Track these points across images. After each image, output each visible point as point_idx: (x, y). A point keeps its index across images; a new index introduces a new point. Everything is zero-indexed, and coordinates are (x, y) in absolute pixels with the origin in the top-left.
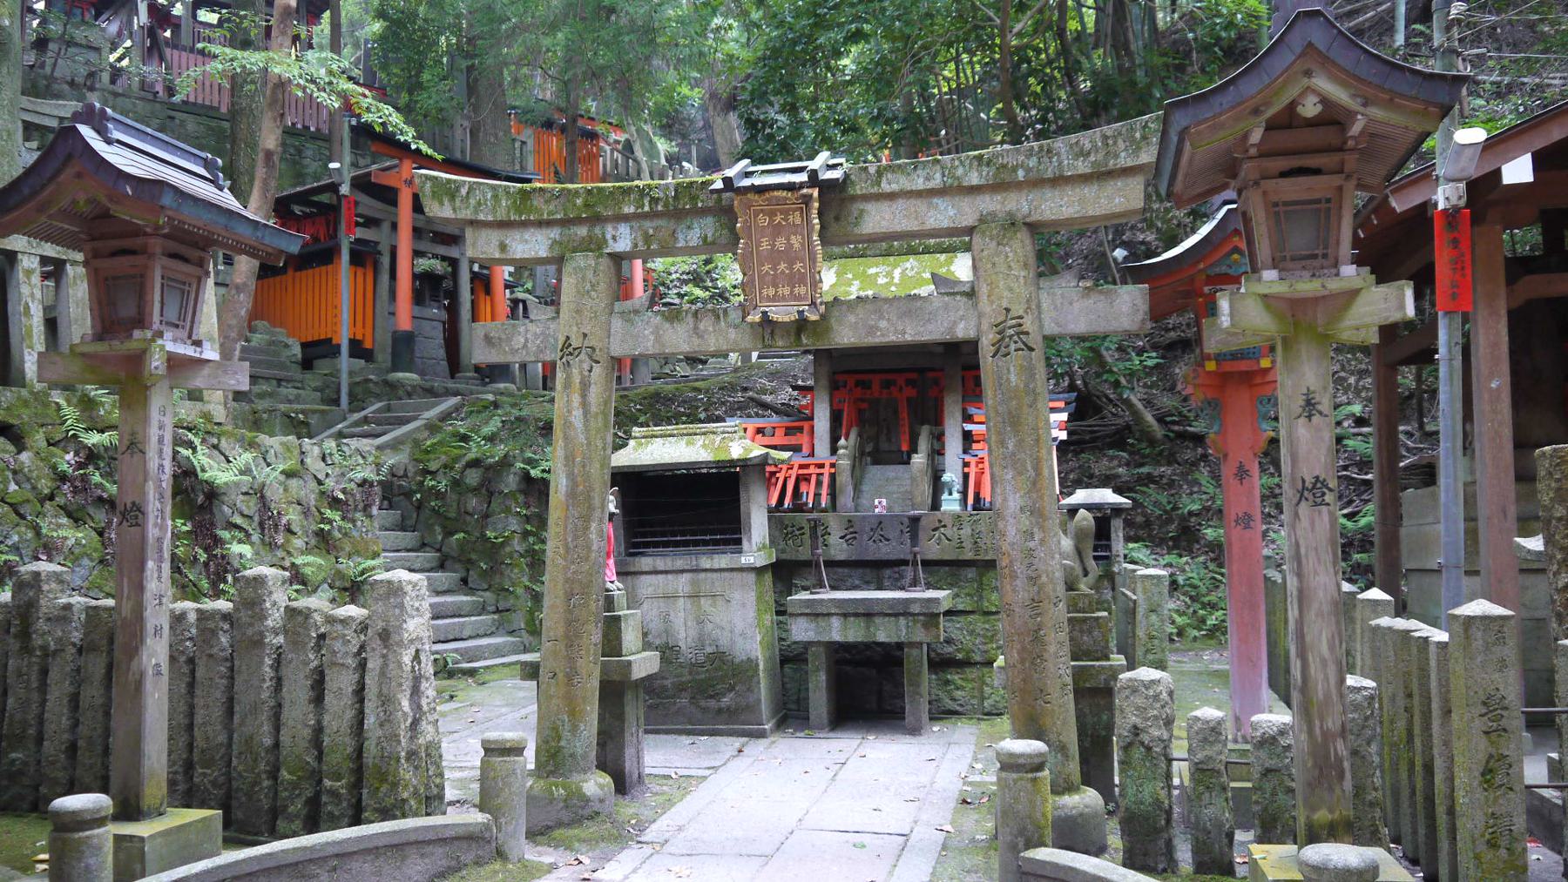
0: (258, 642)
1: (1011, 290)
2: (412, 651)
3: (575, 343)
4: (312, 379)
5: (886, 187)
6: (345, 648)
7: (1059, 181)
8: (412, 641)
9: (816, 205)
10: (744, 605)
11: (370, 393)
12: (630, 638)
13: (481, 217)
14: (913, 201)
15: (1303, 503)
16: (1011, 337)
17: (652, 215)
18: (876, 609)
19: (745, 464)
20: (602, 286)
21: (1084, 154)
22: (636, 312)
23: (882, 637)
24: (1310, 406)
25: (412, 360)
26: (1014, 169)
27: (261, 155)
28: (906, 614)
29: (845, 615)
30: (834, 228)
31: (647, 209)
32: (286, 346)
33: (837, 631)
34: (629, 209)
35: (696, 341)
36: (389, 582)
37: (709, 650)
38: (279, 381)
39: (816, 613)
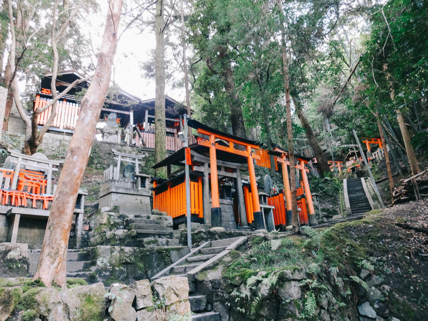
4: (177, 234)
11: (202, 239)
25: (221, 221)
32: (166, 219)
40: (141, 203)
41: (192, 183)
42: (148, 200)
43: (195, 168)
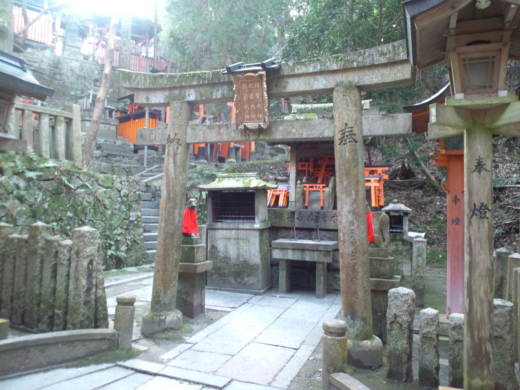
0: (35, 252)
1: (348, 115)
2: (88, 260)
3: (172, 137)
4: (136, 157)
5: (297, 72)
6: (64, 256)
7: (372, 67)
8: (88, 256)
9: (265, 79)
10: (255, 243)
11: (154, 161)
12: (200, 255)
13: (140, 87)
14: (308, 77)
15: (474, 217)
16: (347, 136)
17: (203, 85)
18: (306, 248)
19: (256, 189)
20: (184, 114)
21: (383, 54)
22: (197, 125)
23: (307, 259)
24: (479, 166)
26: (352, 62)
27: (104, 75)
28: (317, 250)
29: (294, 249)
30: (275, 90)
31: (201, 83)
32: (129, 145)
33: (291, 255)
34: (195, 83)
35: (219, 137)
36: (80, 231)
37: (241, 260)
38: (124, 157)
39: (283, 248)
40: (109, 130)
41: (151, 119)
42: (114, 128)
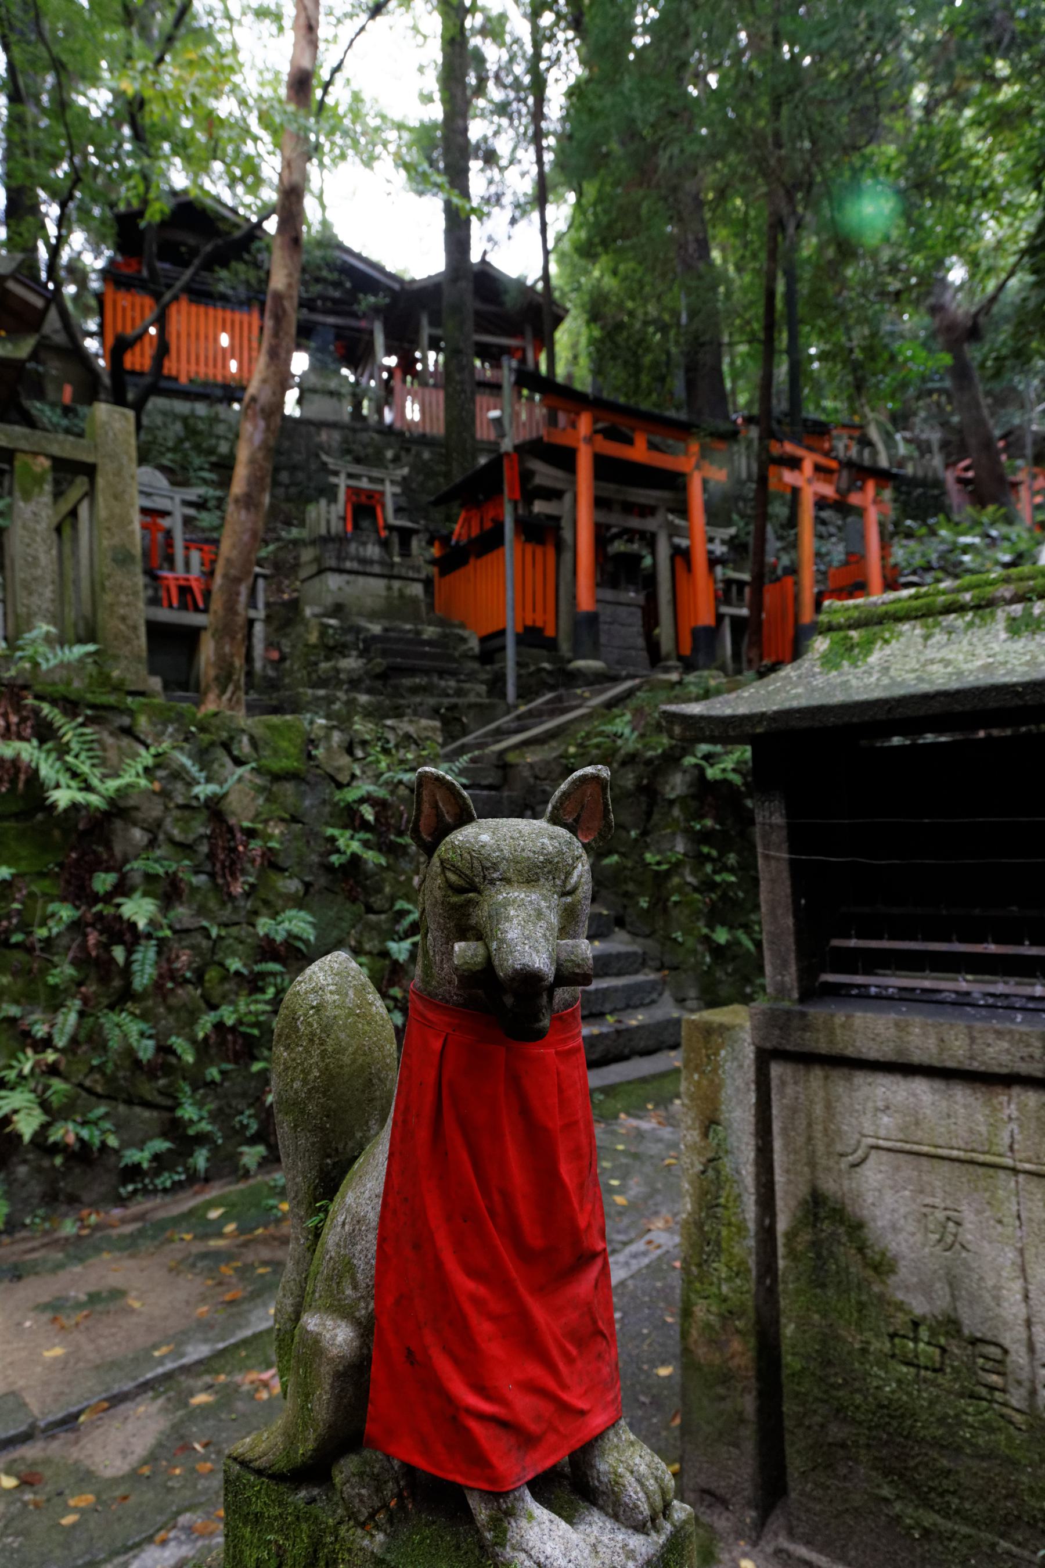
41: (529, 548)
43: (539, 507)
